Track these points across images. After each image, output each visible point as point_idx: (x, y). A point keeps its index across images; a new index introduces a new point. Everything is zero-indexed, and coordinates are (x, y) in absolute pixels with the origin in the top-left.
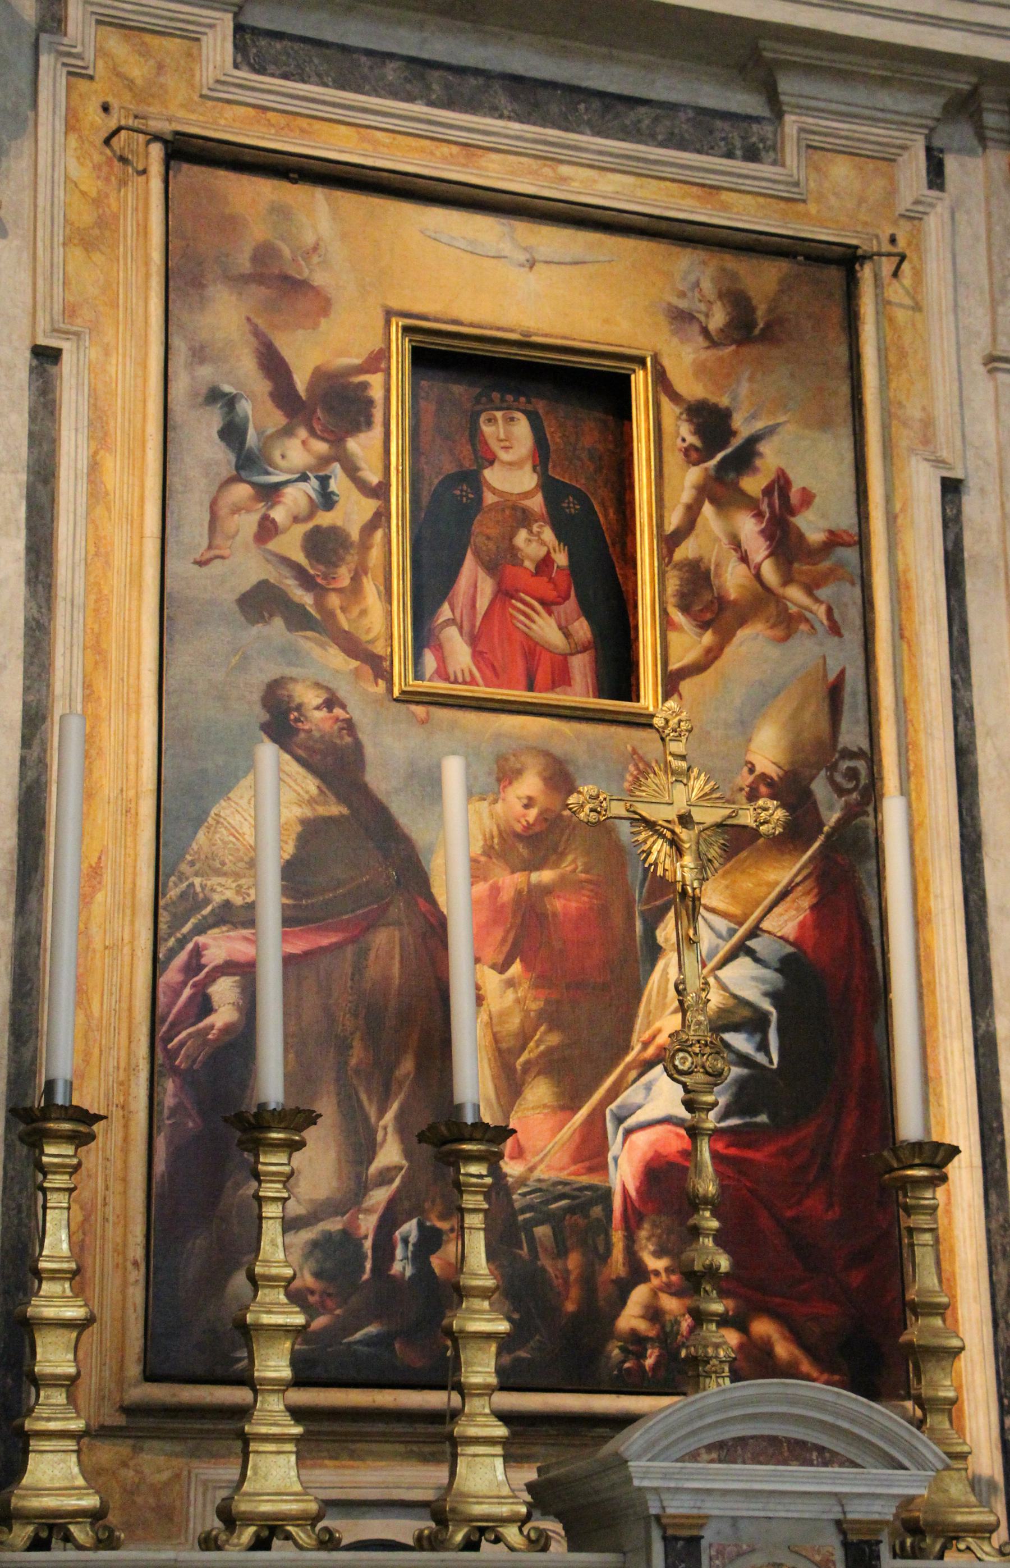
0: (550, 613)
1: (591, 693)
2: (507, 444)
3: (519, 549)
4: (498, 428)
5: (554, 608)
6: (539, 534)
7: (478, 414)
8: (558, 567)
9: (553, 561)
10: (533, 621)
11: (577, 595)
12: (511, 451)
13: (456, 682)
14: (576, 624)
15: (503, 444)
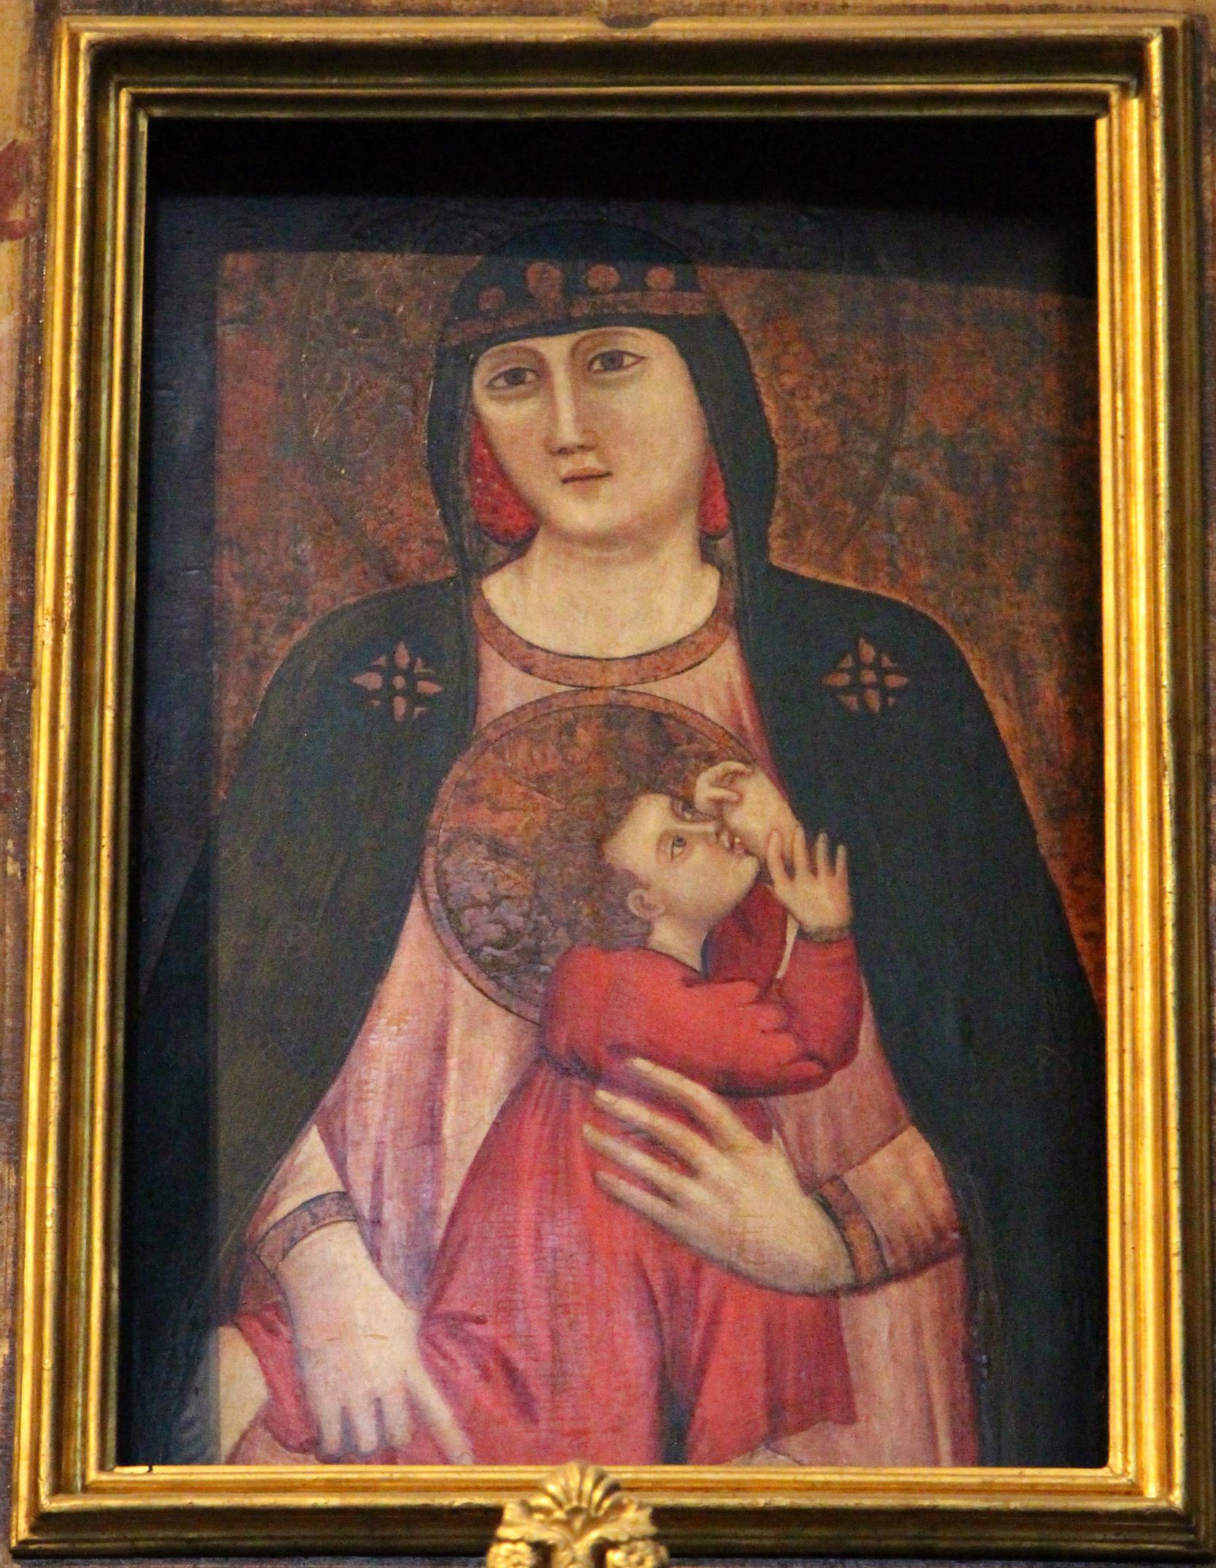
0: (763, 1129)
1: (945, 1445)
2: (590, 462)
3: (632, 880)
4: (552, 402)
5: (783, 1105)
6: (719, 810)
7: (465, 360)
8: (802, 934)
9: (784, 913)
10: (688, 1168)
11: (886, 1043)
12: (605, 487)
13: (348, 1454)
14: (882, 1160)
15: (567, 466)
